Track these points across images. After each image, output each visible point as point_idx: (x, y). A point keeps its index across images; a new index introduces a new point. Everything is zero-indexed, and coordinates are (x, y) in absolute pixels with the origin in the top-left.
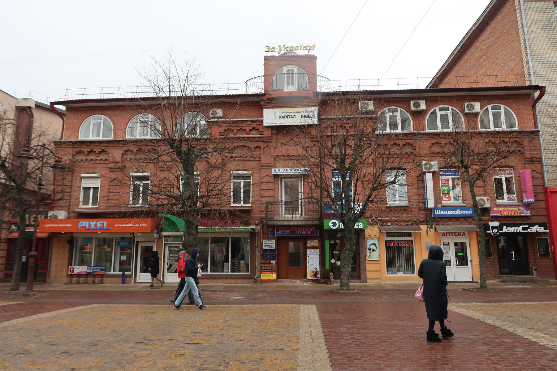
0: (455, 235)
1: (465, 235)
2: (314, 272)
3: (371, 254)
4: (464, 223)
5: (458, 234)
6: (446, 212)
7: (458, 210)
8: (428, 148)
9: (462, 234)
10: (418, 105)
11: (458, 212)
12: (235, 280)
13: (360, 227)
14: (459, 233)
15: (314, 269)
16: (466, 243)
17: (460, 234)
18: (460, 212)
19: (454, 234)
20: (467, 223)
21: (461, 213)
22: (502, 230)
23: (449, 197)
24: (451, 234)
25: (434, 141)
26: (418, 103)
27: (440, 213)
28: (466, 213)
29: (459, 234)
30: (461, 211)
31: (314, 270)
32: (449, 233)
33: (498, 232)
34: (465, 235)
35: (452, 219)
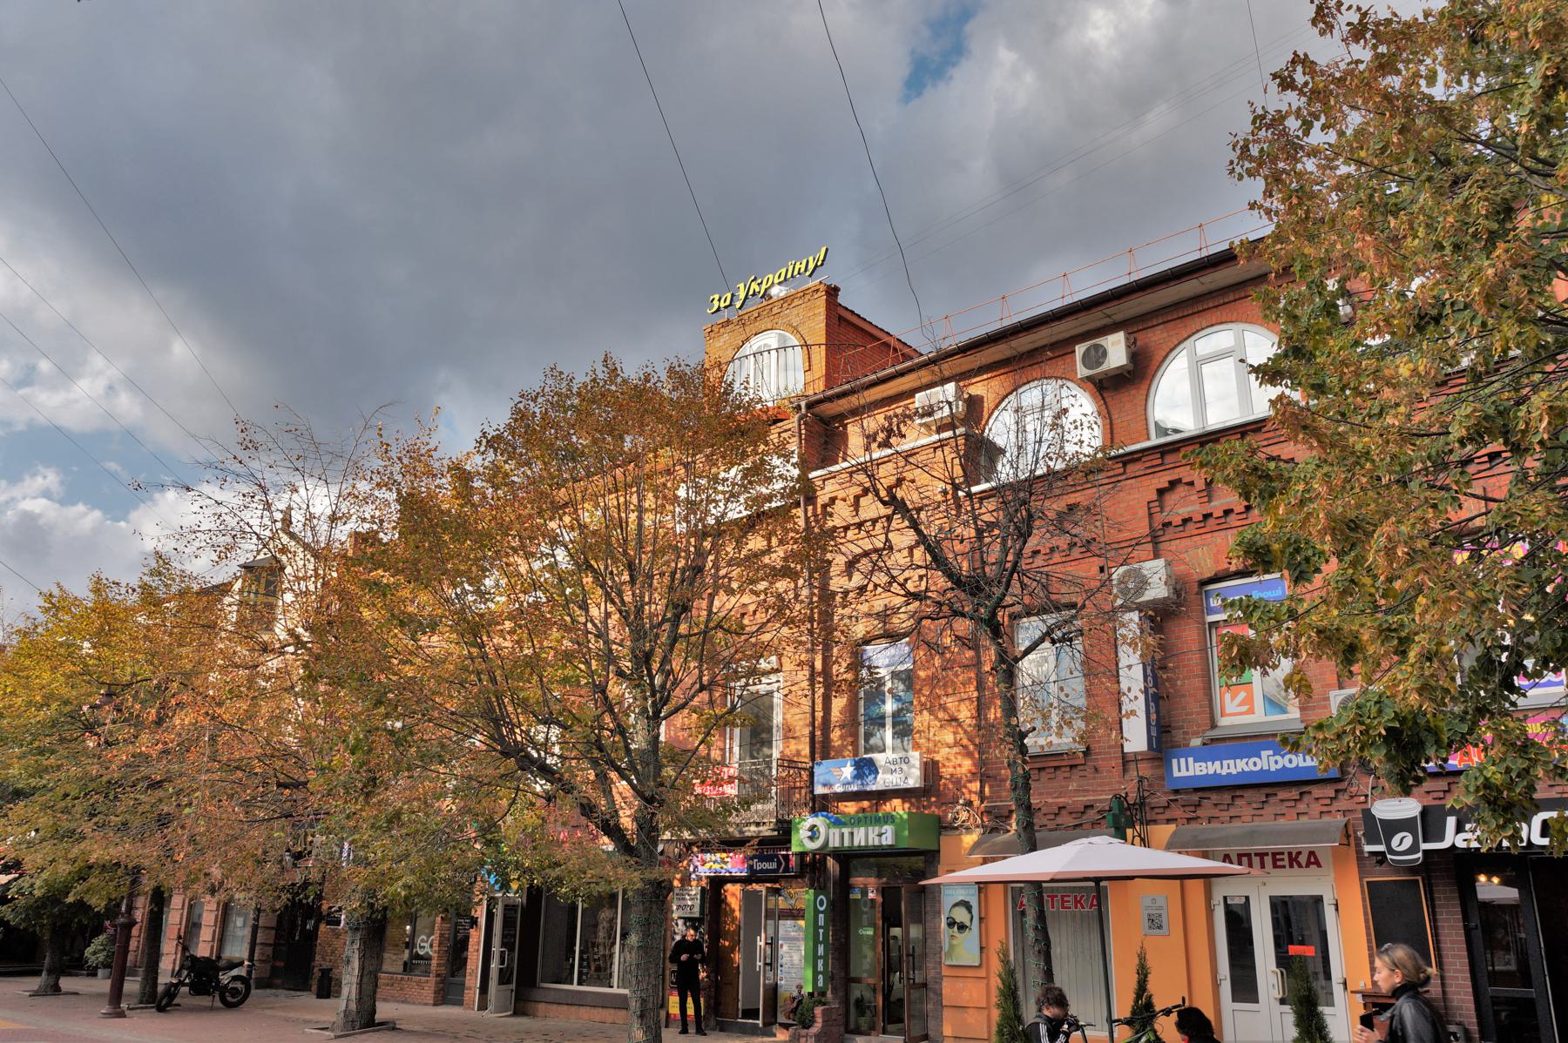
0: (1275, 866)
1: (1319, 865)
2: (794, 998)
3: (955, 942)
4: (1302, 807)
5: (1286, 857)
6: (1217, 763)
7: (1264, 754)
8: (1143, 512)
9: (1303, 859)
10: (1097, 352)
11: (1268, 762)
12: (612, 1011)
13: (884, 843)
14: (1290, 854)
15: (794, 988)
16: (1318, 900)
17: (1296, 859)
18: (1272, 759)
19: (1268, 860)
20: (1316, 808)
21: (1279, 766)
22: (1441, 838)
23: (1249, 700)
24: (1256, 860)
25: (1162, 480)
26: (1097, 347)
27: (1191, 773)
28: (1302, 764)
29: (1294, 860)
30: (1278, 758)
31: (795, 994)
32: (1248, 855)
33: (1414, 848)
34: (1319, 865)
35: (1248, 794)
